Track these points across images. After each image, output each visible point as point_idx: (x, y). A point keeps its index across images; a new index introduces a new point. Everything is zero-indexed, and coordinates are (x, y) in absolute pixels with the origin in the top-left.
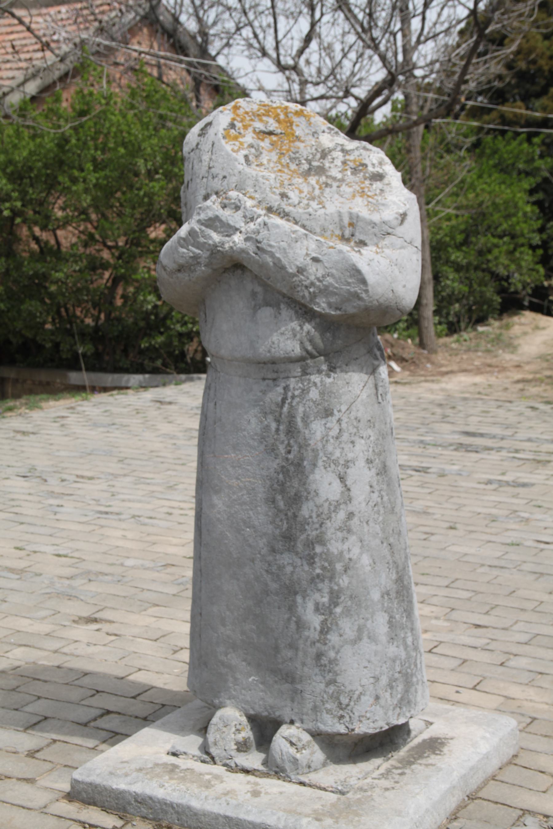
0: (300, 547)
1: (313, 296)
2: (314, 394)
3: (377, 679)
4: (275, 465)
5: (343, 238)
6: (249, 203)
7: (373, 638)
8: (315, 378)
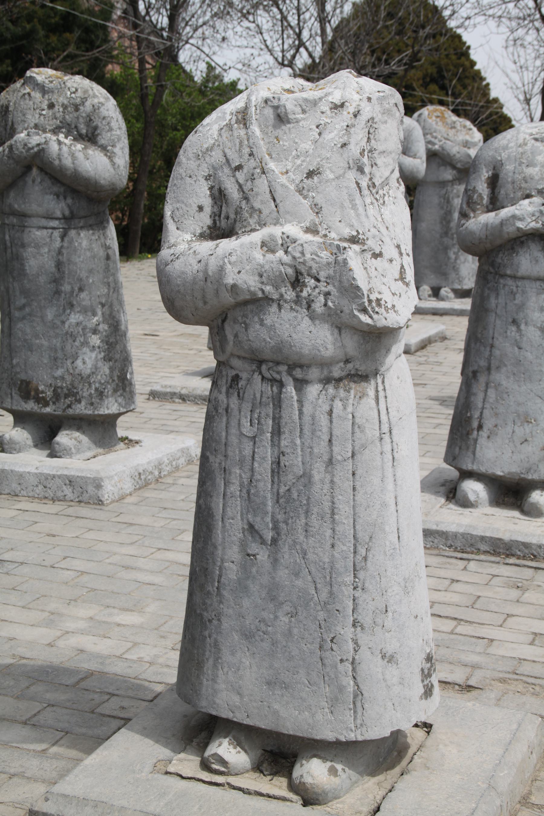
0: (450, 235)
1: (457, 163)
2: (455, 191)
3: (469, 274)
4: (442, 212)
5: (465, 147)
6: (439, 137)
7: (468, 262)
8: (455, 187)
